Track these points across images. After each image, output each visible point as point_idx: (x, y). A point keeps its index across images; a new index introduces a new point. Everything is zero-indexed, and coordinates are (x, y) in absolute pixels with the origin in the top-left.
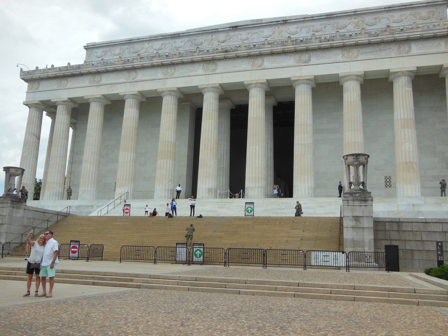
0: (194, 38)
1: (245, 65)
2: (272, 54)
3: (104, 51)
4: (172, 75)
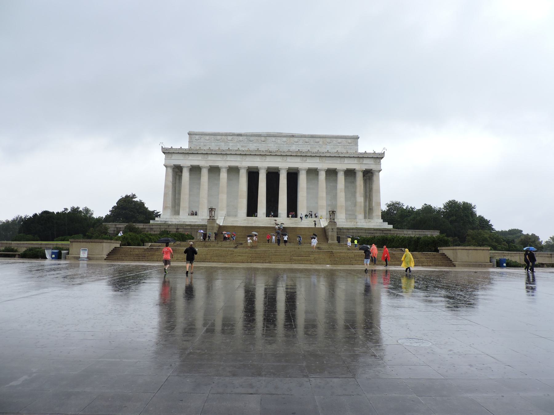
2: (291, 156)
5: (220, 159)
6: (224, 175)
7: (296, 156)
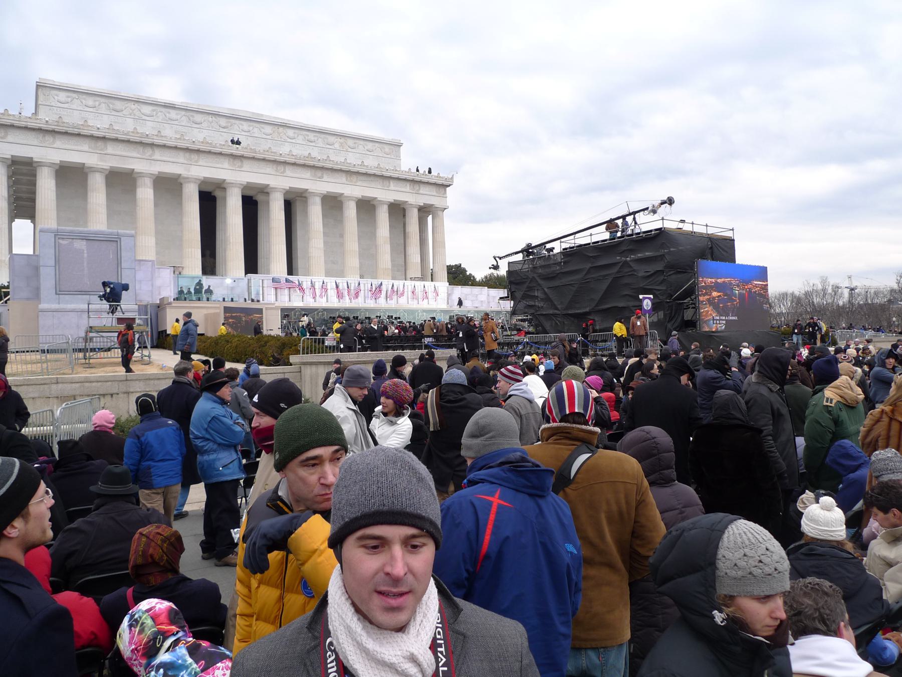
0: (191, 114)
1: (270, 169)
3: (68, 97)
4: (197, 162)
5: (135, 154)
6: (146, 193)
7: (304, 166)
